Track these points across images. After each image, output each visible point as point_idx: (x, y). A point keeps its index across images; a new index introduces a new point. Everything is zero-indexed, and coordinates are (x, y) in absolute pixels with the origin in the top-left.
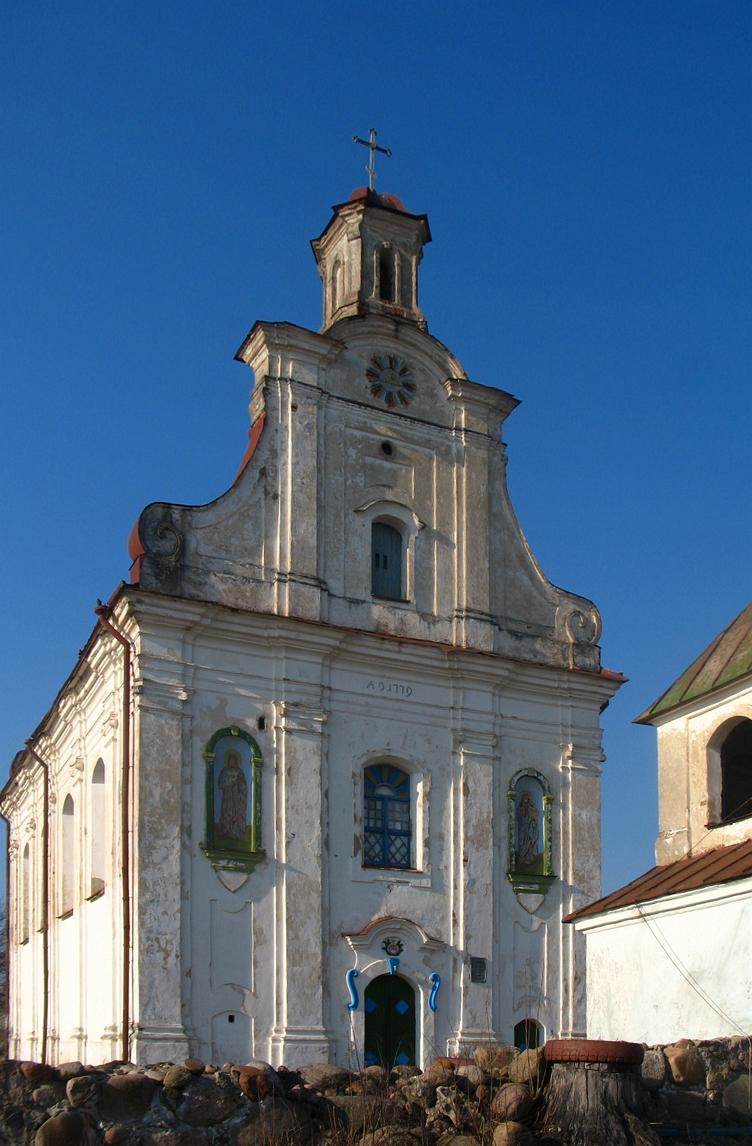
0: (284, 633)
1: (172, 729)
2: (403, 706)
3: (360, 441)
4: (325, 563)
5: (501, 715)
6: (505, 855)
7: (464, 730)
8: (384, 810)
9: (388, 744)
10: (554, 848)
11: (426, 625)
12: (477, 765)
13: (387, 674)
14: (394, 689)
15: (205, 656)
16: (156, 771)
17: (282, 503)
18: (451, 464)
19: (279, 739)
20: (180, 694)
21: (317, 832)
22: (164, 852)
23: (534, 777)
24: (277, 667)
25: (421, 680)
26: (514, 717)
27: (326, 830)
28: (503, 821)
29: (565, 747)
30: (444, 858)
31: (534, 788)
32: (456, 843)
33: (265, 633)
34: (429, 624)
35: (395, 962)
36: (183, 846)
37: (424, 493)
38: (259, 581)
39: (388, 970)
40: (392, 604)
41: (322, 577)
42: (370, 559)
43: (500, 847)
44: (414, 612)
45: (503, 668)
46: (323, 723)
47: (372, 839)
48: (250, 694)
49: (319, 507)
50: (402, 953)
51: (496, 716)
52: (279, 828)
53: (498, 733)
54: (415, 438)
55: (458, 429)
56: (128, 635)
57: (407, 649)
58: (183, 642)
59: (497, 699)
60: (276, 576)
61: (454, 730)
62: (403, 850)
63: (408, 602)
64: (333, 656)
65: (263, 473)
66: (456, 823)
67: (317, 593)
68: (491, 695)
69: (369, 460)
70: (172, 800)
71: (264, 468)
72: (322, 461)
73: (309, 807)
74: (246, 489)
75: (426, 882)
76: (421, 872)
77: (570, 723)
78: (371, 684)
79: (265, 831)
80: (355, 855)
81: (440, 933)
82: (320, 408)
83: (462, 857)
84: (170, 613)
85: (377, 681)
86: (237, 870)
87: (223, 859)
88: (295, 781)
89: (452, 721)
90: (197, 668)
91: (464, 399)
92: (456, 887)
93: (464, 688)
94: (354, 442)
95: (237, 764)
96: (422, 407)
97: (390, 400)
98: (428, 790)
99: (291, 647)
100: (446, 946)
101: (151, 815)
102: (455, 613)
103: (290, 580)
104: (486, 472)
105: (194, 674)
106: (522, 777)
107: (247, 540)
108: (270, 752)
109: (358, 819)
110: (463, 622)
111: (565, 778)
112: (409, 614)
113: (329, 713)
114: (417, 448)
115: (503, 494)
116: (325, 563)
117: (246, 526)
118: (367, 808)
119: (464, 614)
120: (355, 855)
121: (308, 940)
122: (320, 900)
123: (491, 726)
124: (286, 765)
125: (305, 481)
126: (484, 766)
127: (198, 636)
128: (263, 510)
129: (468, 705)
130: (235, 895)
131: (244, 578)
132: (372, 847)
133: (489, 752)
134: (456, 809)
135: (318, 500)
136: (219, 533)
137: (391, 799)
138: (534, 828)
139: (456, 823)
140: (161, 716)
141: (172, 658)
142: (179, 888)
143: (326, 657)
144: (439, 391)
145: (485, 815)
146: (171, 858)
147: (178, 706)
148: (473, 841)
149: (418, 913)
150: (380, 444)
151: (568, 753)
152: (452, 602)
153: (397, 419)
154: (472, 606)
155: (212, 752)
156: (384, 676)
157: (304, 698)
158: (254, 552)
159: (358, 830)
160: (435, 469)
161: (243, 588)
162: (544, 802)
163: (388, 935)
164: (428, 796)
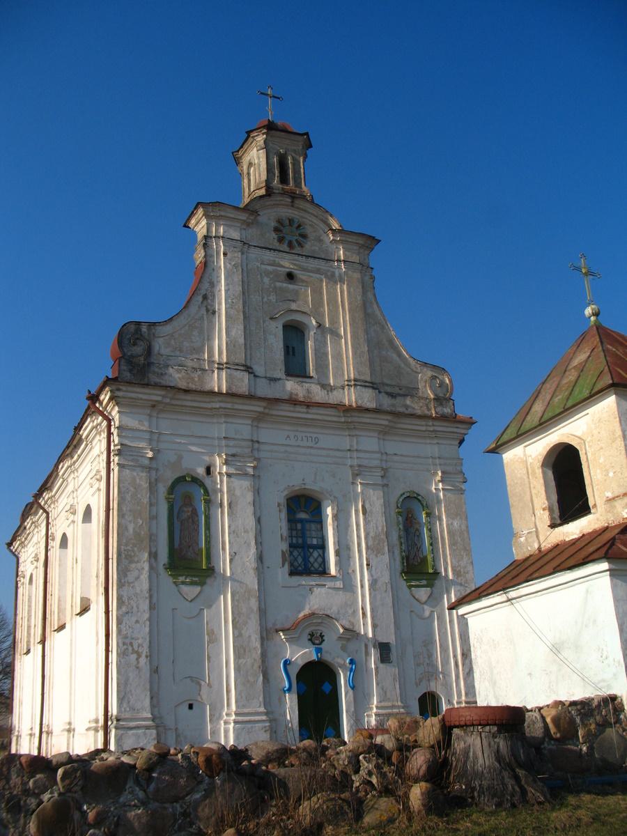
0: (223, 405)
1: (142, 479)
2: (313, 451)
3: (271, 273)
4: (251, 354)
5: (386, 453)
6: (398, 558)
7: (360, 466)
8: (303, 529)
9: (303, 480)
10: (435, 551)
11: (326, 393)
12: (371, 491)
13: (300, 429)
14: (305, 439)
15: (166, 425)
16: (130, 511)
17: (219, 316)
18: (336, 283)
20: (147, 453)
21: (253, 550)
22: (136, 573)
23: (415, 498)
24: (218, 429)
25: (326, 431)
28: (394, 533)
29: (435, 474)
30: (352, 564)
31: (416, 506)
33: (209, 406)
34: (328, 391)
35: (319, 651)
36: (151, 568)
37: (318, 303)
38: (204, 370)
39: (314, 657)
40: (300, 379)
41: (249, 364)
42: (283, 350)
43: (393, 552)
44: (317, 384)
45: (384, 419)
46: (254, 468)
47: (295, 553)
48: (199, 450)
49: (245, 317)
50: (324, 643)
51: (382, 454)
52: (224, 549)
53: (385, 467)
54: (310, 268)
55: (338, 261)
56: (110, 413)
57: (314, 410)
58: (150, 416)
59: (382, 442)
60: (216, 366)
61: (351, 466)
62: (320, 560)
63: (312, 377)
64: (259, 419)
65: (205, 297)
66: (359, 537)
67: (246, 375)
68: (377, 440)
69: (278, 284)
70: (143, 533)
71: (206, 294)
72: (246, 288)
73: (246, 531)
74: (193, 309)
75: (339, 584)
77: (437, 455)
78: (288, 437)
79: (213, 551)
80: (283, 566)
81: (353, 624)
82: (243, 254)
83: (365, 563)
84: (140, 396)
86: (193, 583)
87: (182, 576)
88: (235, 512)
89: (349, 460)
90: (160, 434)
91: (341, 242)
92: (362, 586)
93: (356, 435)
94: (268, 273)
96: (313, 248)
97: (290, 245)
98: (335, 512)
99: (228, 414)
100: (358, 634)
101: (126, 545)
102: (346, 383)
103: (226, 368)
104: (361, 287)
105: (158, 438)
108: (216, 491)
109: (284, 538)
110: (352, 389)
111: (438, 496)
112: (313, 385)
113: (258, 459)
114: (311, 274)
116: (251, 354)
117: (194, 333)
118: (291, 529)
119: (353, 383)
120: (283, 566)
121: (250, 636)
122: (257, 603)
123: (379, 462)
124: (228, 500)
125: (234, 301)
126: (376, 492)
128: (206, 322)
129: (360, 448)
130: (192, 604)
131: (193, 368)
132: (296, 559)
133: (379, 481)
134: (358, 525)
135: (244, 313)
136: (174, 339)
137: (307, 521)
139: (359, 537)
140: (134, 470)
141: (142, 428)
142: (148, 601)
143: (254, 419)
144: (324, 237)
145: (380, 528)
146: (142, 577)
147: (147, 462)
148: (372, 550)
149: (335, 609)
150: (285, 274)
151: (438, 478)
152: (343, 374)
153: (296, 257)
154: (358, 377)
155: (172, 494)
156: (297, 431)
158: (200, 350)
159: (284, 546)
160: (325, 287)
161: (193, 375)
162: (424, 516)
163: (313, 628)
164: (335, 517)
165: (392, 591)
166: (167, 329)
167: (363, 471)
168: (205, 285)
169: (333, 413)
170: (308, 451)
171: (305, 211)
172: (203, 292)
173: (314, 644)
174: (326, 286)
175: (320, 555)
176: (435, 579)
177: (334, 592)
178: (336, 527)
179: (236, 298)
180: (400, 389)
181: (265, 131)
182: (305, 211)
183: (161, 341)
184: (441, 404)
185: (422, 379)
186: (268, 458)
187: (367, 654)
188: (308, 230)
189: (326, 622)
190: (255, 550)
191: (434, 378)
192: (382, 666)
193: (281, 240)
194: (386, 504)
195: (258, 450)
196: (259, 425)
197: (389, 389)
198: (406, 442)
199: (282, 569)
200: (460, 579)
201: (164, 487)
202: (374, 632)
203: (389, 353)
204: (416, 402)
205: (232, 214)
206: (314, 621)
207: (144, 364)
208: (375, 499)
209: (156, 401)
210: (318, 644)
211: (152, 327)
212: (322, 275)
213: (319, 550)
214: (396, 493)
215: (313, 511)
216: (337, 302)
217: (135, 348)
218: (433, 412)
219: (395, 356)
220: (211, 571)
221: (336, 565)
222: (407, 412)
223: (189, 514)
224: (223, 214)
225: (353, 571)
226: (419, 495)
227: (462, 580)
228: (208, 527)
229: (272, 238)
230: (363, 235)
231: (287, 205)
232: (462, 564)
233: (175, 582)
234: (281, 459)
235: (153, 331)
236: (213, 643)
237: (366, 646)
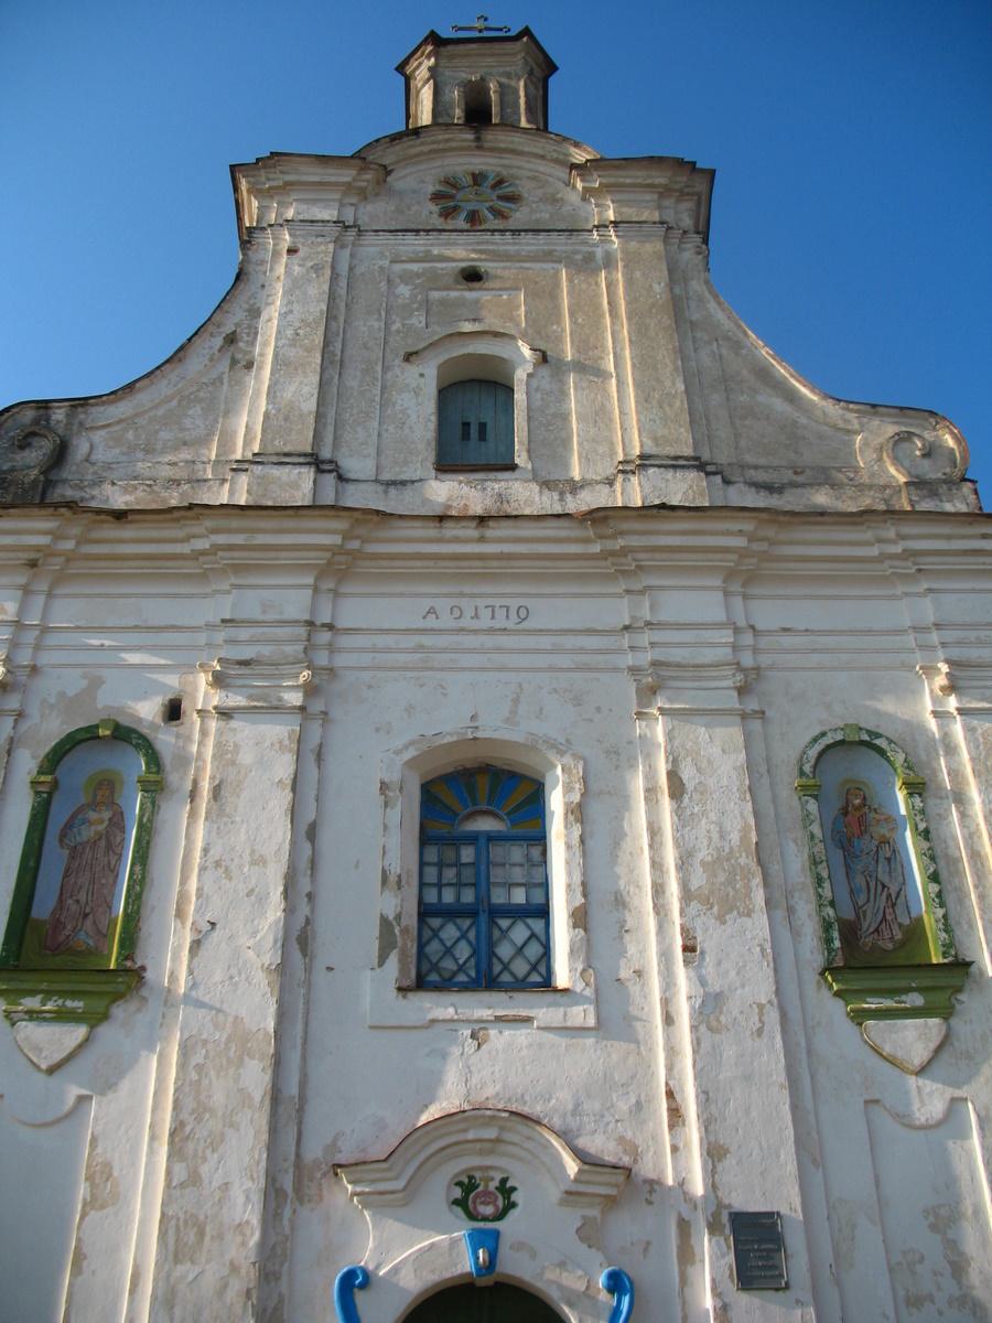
0: (221, 539)
2: (504, 640)
3: (418, 275)
5: (752, 627)
7: (654, 664)
9: (473, 718)
10: (950, 898)
13: (467, 589)
19: (204, 733)
21: (274, 912)
23: (862, 743)
26: (785, 630)
27: (304, 910)
28: (791, 848)
29: (930, 670)
30: (632, 950)
31: (865, 768)
32: (660, 909)
33: (185, 549)
34: (562, 494)
35: (488, 1241)
39: (464, 1262)
43: (790, 910)
50: (513, 1214)
51: (737, 631)
64: (337, 570)
69: (435, 295)
74: (195, 363)
75: (582, 1015)
76: (565, 991)
78: (432, 611)
79: (148, 926)
80: (381, 964)
81: (633, 1150)
83: (679, 942)
85: (443, 605)
86: (62, 1016)
87: (32, 993)
91: (607, 188)
92: (669, 1020)
94: (406, 278)
95: (112, 792)
97: (473, 218)
98: (576, 798)
100: (654, 1185)
105: (39, 639)
106: (828, 747)
107: (188, 429)
108: (183, 760)
109: (393, 879)
111: (946, 738)
112: (517, 485)
115: (707, 293)
120: (381, 964)
121: (226, 1186)
122: (267, 1078)
123: (729, 650)
124: (212, 778)
125: (301, 332)
126: (719, 732)
127: (60, 579)
128: (225, 387)
129: (663, 617)
133: (732, 700)
134: (654, 831)
137: (492, 838)
138: (889, 860)
139: (657, 865)
145: (735, 837)
149: (563, 1098)
151: (941, 681)
152: (613, 453)
153: (487, 237)
154: (651, 449)
156: (462, 595)
157: (266, 651)
158: (204, 441)
159: (400, 905)
162: (901, 796)
163: (474, 1161)
164: (577, 812)
165: (784, 1032)
166: (123, 409)
167: (675, 678)
168: (234, 318)
169: (563, 533)
170: (489, 641)
171: (514, 152)
172: (228, 329)
173: (472, 1216)
174: (570, 280)
175: (533, 936)
176: (959, 990)
177: (561, 1041)
178: (576, 840)
179: (309, 325)
181: (430, 48)
182: (514, 152)
183: (98, 437)
185: (865, 443)
186: (363, 669)
187: (687, 1255)
188: (525, 188)
189: (515, 1138)
190: (280, 914)
191: (903, 438)
192: (744, 1301)
193: (447, 214)
194: (757, 770)
195: (332, 648)
196: (342, 590)
197: (761, 476)
199: (378, 970)
201: (34, 757)
202: (711, 1174)
203: (760, 398)
204: (851, 498)
205: (314, 174)
206: (471, 1135)
207: (35, 482)
208: (715, 751)
209: (38, 549)
210: (485, 1219)
211: (80, 409)
212: (560, 262)
213: (530, 921)
214: (794, 740)
215: (518, 807)
216: (598, 307)
217: (26, 453)
219: (779, 404)
220: (128, 980)
221: (572, 952)
223: (101, 828)
224: (288, 178)
225: (639, 973)
226: (879, 736)
228: (142, 856)
229: (425, 212)
230: (661, 160)
231: (468, 148)
233: (8, 1015)
234: (406, 669)
235: (82, 416)
236: (102, 1207)
237: (684, 1227)
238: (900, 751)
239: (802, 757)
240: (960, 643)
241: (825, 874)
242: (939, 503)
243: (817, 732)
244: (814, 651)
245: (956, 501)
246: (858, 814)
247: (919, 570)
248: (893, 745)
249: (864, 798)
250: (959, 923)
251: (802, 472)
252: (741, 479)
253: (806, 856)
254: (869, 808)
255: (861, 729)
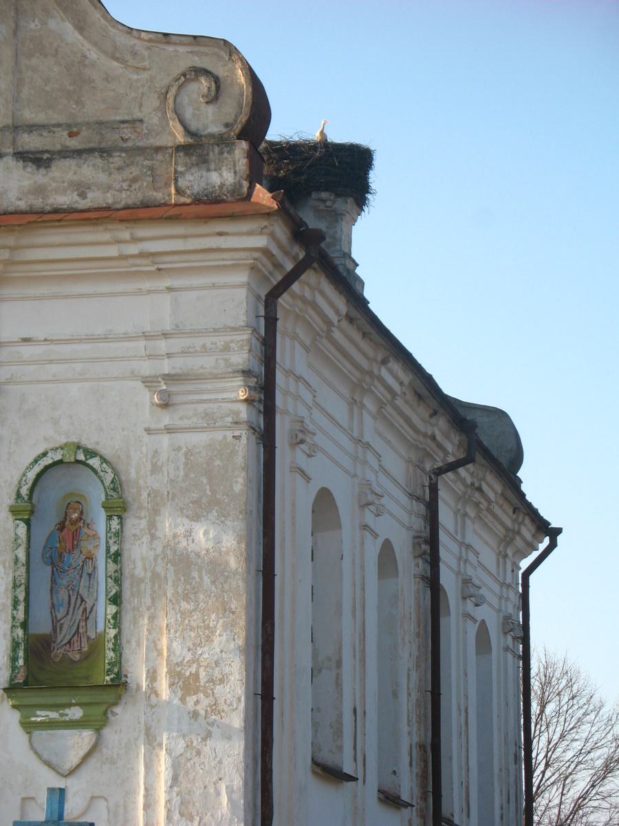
23: (78, 462)
26: (26, 340)
106: (47, 468)
138: (90, 575)
180: (71, 135)
184: (204, 162)
197: (31, 142)
198: (66, 297)
200: (191, 700)
218: (173, 191)
222: (82, 204)
226: (91, 453)
227: (197, 703)
232: (207, 654)
238: (109, 471)
239: (22, 479)
240: (185, 352)
241: (21, 597)
242: (204, 173)
243: (41, 451)
244: (51, 362)
245: (224, 168)
246: (73, 528)
247: (159, 270)
248: (104, 465)
249: (82, 513)
250: (129, 642)
251: (77, 134)
252: (11, 150)
253: (11, 579)
254: (84, 523)
255: (79, 447)
